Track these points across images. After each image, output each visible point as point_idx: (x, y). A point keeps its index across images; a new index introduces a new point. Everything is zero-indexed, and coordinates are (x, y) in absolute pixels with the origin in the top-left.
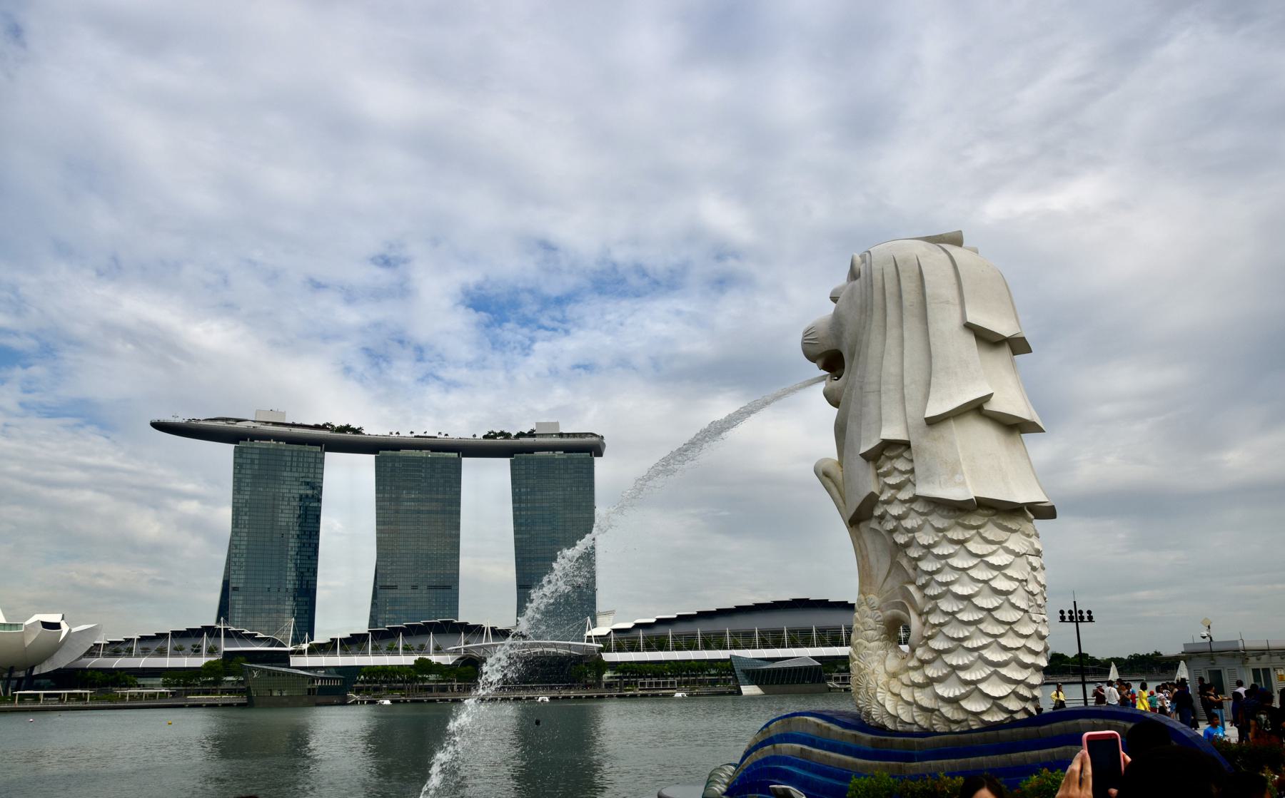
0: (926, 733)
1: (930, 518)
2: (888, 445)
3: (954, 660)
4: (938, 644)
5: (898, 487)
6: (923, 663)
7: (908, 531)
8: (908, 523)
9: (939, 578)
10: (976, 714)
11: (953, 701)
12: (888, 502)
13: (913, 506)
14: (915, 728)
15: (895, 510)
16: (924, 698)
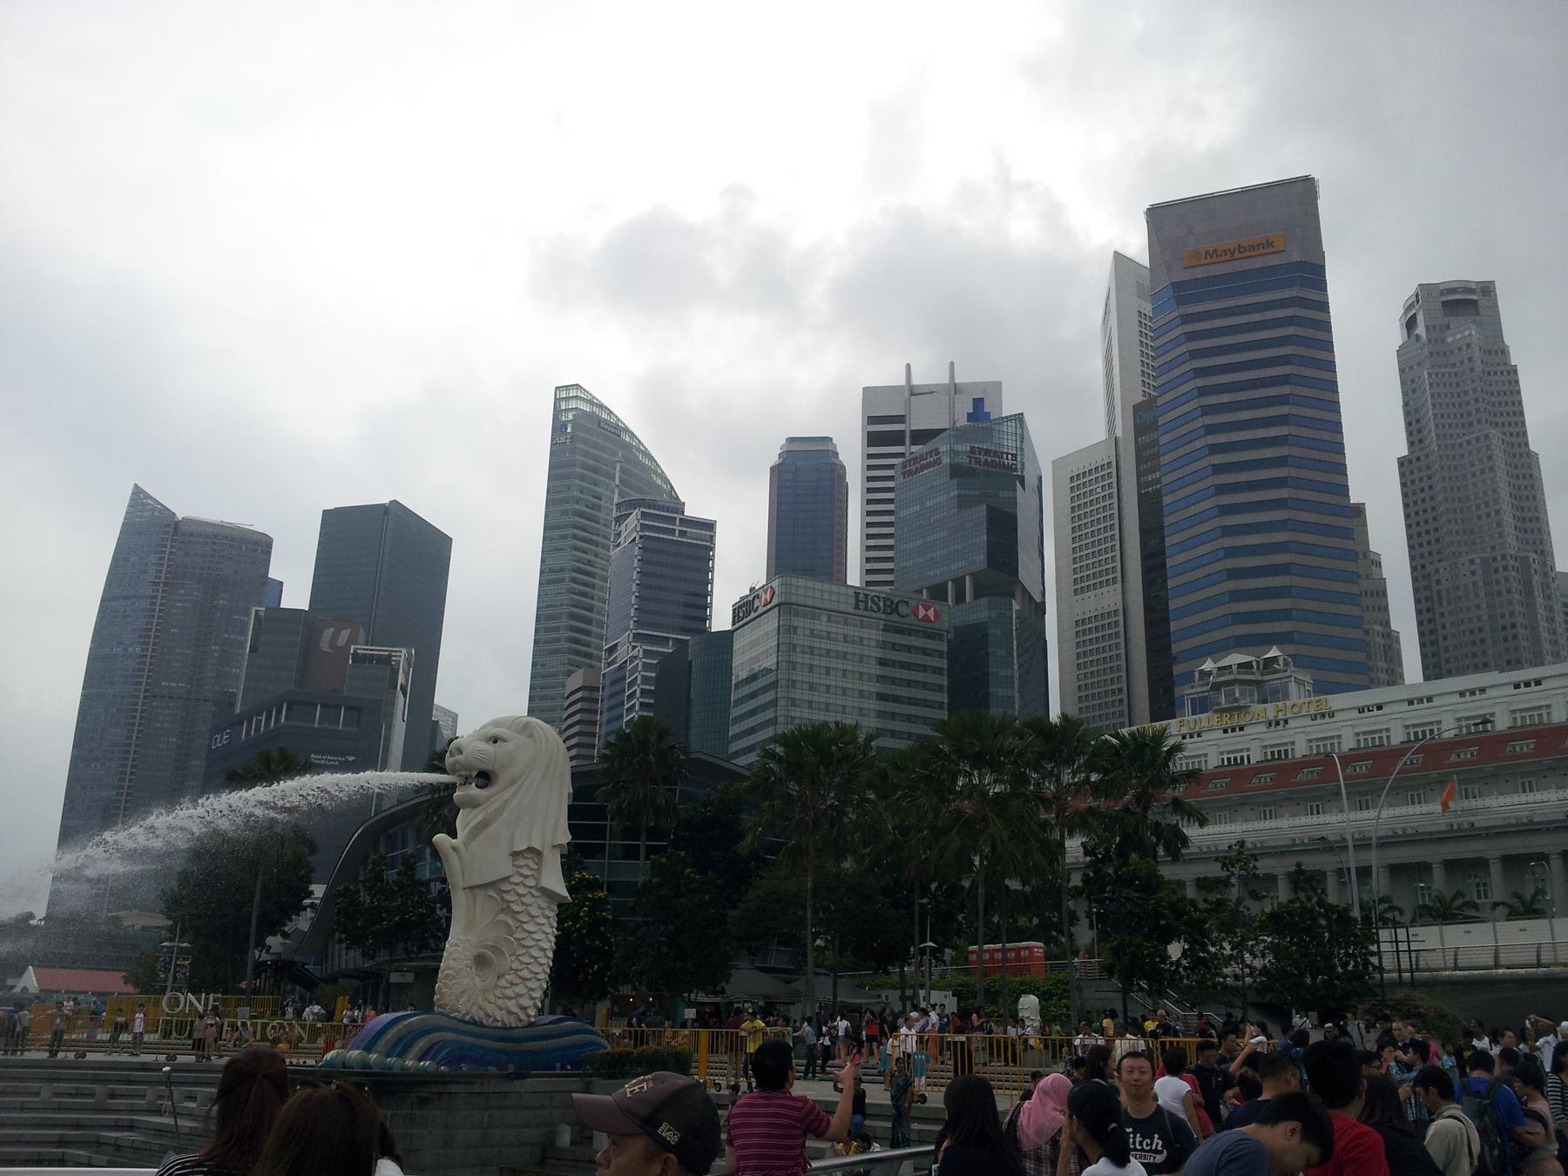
0: (504, 1028)
1: (538, 900)
2: (530, 850)
3: (530, 984)
4: (525, 974)
5: (526, 877)
6: (512, 984)
7: (524, 904)
8: (525, 900)
9: (534, 936)
10: (529, 1016)
11: (524, 1009)
12: (516, 884)
13: (533, 891)
14: (500, 1024)
15: (521, 890)
16: (512, 1005)
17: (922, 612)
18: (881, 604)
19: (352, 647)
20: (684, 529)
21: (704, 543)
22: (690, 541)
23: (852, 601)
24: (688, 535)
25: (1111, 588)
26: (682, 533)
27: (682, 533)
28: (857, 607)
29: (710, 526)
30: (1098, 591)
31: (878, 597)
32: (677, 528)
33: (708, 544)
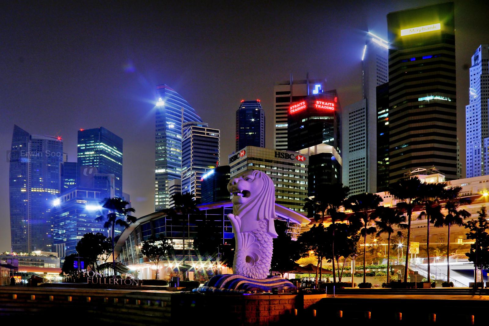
17: (299, 158)
18: (285, 155)
19: (94, 174)
20: (208, 132)
21: (216, 137)
22: (211, 136)
23: (274, 154)
24: (210, 134)
25: (362, 150)
26: (208, 134)
27: (208, 134)
28: (276, 156)
29: (218, 132)
30: (358, 151)
31: (284, 153)
32: (206, 132)
33: (217, 137)
